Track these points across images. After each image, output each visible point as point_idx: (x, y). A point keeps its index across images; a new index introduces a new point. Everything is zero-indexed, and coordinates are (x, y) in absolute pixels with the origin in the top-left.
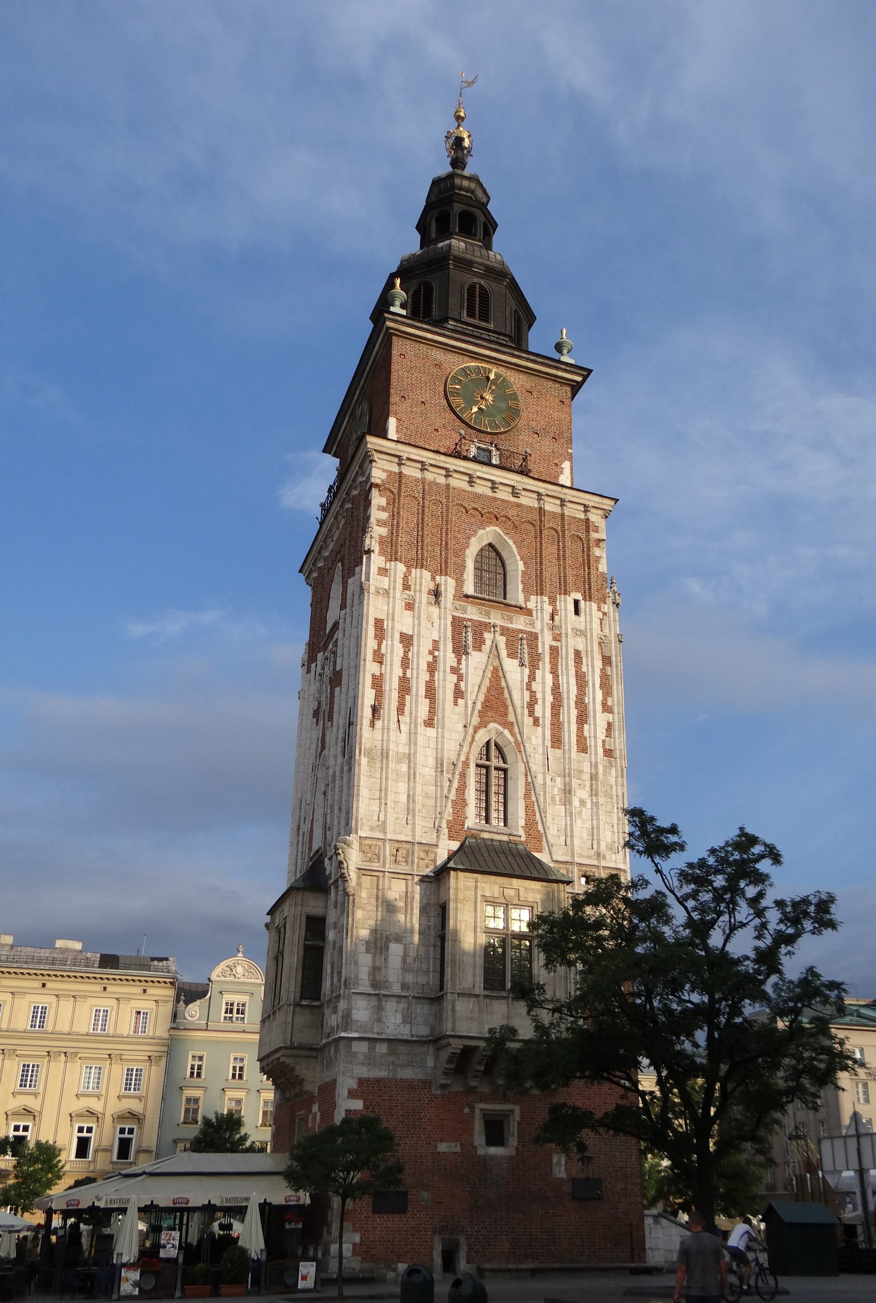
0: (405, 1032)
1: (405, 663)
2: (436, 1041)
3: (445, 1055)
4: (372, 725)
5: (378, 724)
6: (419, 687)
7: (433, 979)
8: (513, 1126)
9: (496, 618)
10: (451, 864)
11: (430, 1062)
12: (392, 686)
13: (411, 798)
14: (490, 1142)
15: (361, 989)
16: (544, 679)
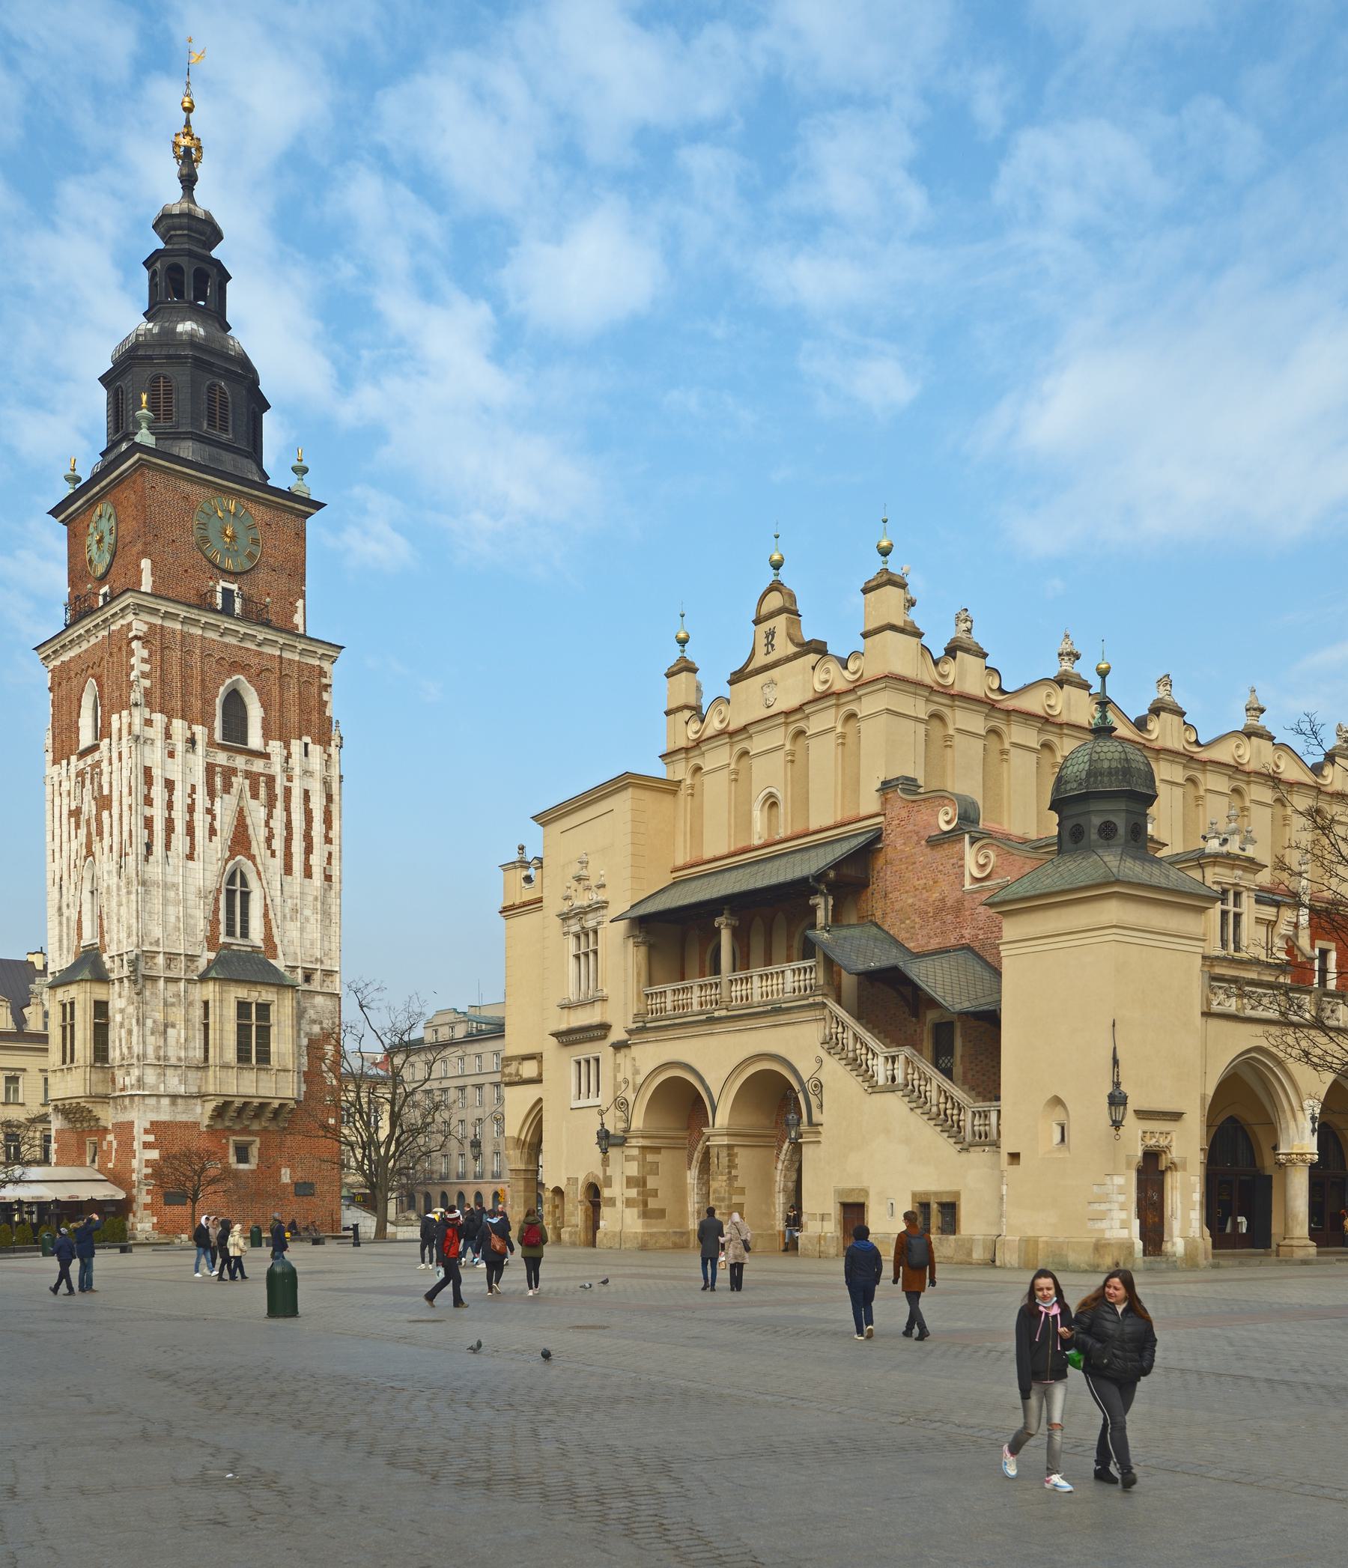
0: (182, 1090)
1: (170, 806)
2: (202, 1096)
3: (210, 1106)
4: (147, 860)
5: (151, 858)
6: (180, 827)
7: (199, 1054)
8: (254, 1151)
9: (240, 762)
10: (213, 974)
11: (199, 1110)
12: (159, 826)
13: (178, 918)
14: (239, 1161)
15: (149, 1061)
16: (279, 812)
